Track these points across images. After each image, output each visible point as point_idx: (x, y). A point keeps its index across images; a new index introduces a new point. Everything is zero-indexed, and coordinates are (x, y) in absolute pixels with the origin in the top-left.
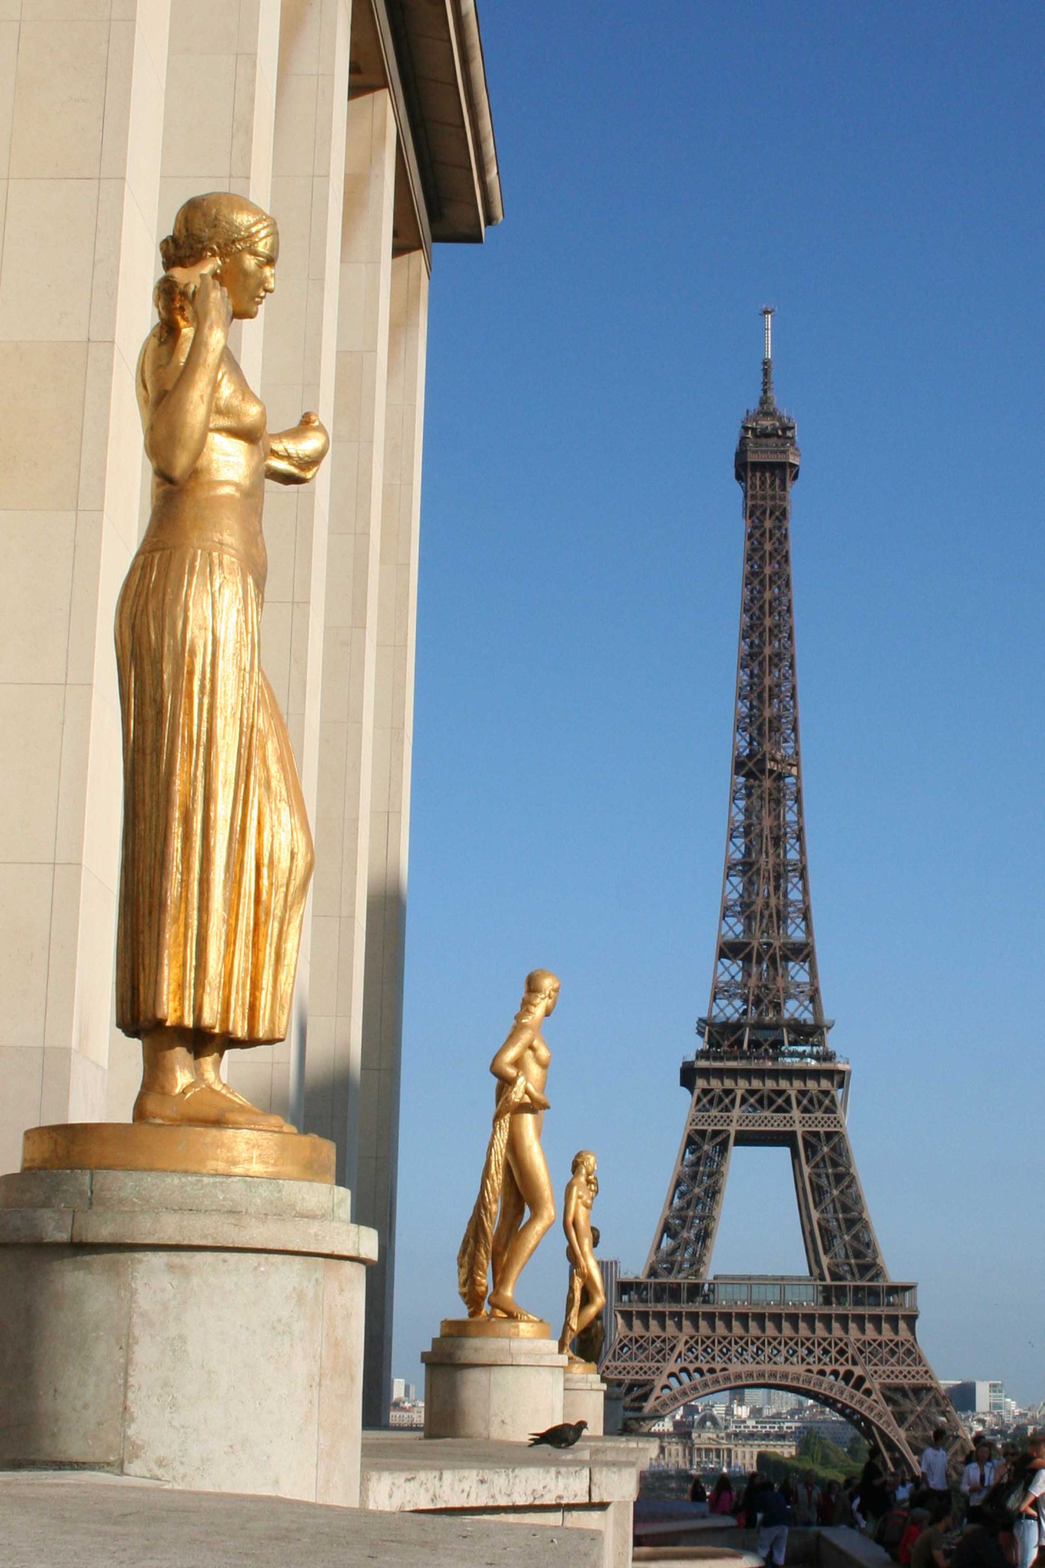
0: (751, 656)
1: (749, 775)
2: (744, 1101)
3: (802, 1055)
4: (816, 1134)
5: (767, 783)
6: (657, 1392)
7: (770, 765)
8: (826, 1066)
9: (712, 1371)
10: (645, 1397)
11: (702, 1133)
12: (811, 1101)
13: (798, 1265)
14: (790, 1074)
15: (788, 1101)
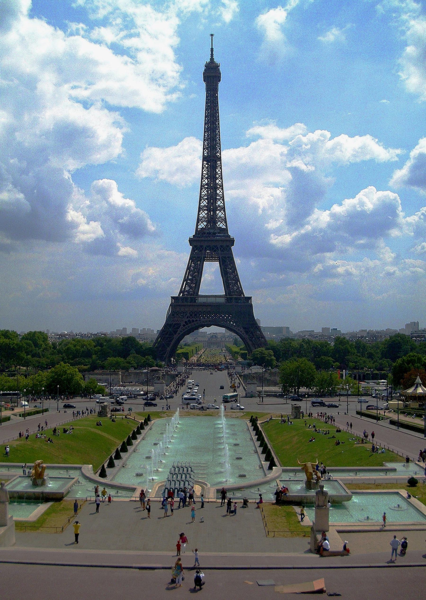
0: (208, 129)
1: (208, 162)
2: (205, 248)
3: (220, 236)
4: (225, 257)
5: (212, 163)
6: (182, 326)
7: (212, 158)
8: (228, 239)
9: (196, 321)
10: (178, 328)
11: (195, 257)
12: (224, 249)
13: (222, 292)
14: (216, 240)
15: (217, 248)
